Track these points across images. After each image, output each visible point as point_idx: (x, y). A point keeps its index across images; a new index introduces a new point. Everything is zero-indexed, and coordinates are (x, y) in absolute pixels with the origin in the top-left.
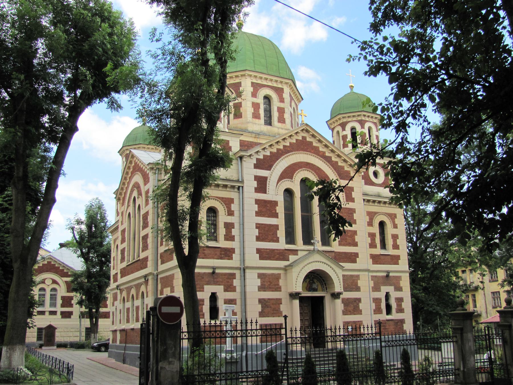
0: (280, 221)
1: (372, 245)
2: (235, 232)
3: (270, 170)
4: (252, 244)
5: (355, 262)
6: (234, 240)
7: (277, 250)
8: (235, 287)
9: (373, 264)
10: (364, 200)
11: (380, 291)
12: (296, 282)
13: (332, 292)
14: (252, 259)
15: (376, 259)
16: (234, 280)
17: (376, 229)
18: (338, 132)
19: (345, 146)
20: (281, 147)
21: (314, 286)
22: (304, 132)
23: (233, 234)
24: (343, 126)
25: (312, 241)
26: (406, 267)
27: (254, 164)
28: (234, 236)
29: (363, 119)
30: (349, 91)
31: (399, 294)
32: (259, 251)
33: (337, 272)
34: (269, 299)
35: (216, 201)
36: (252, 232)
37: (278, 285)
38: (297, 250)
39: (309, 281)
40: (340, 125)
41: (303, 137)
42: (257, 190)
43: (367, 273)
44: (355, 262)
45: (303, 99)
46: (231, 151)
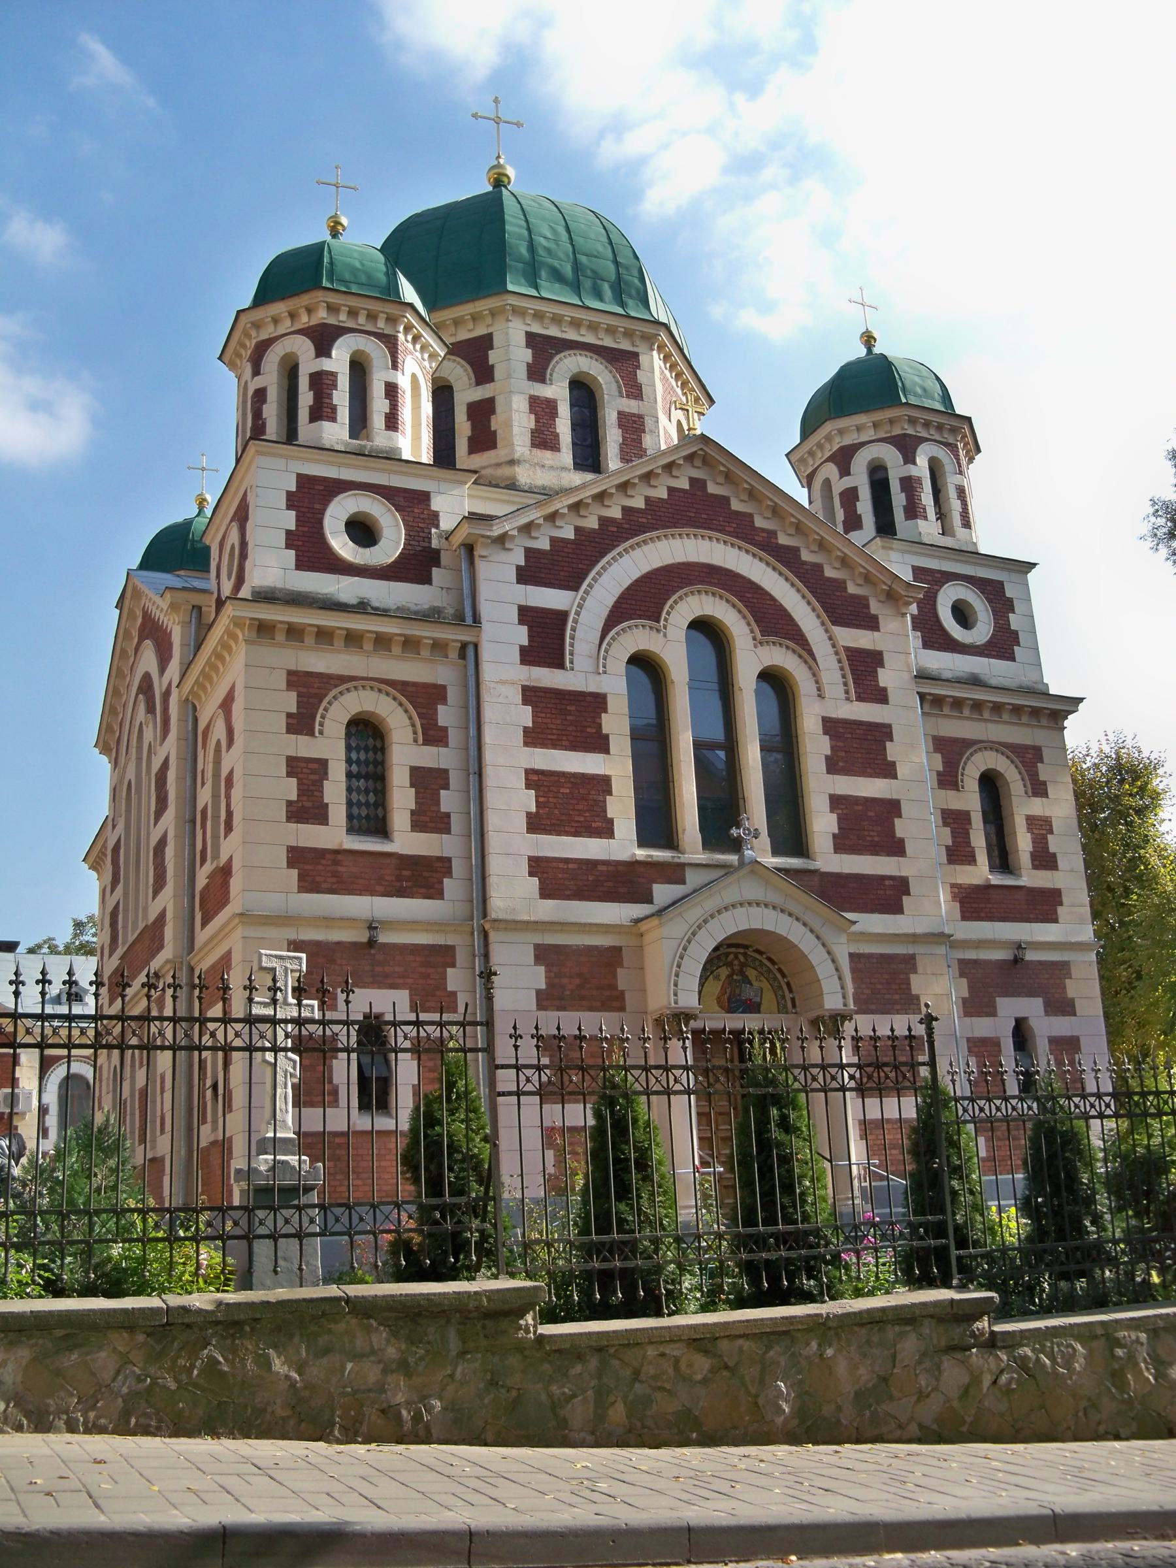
0: (617, 766)
1: (959, 853)
3: (576, 589)
4: (512, 841)
5: (898, 909)
6: (447, 830)
10: (922, 696)
11: (993, 1014)
12: (673, 972)
13: (813, 1014)
14: (513, 891)
15: (975, 903)
16: (450, 971)
17: (970, 799)
18: (827, 483)
19: (853, 522)
20: (616, 513)
21: (748, 993)
22: (698, 462)
23: (444, 809)
24: (843, 459)
25: (734, 832)
26: (1087, 933)
27: (519, 568)
28: (448, 815)
29: (911, 431)
30: (862, 352)
31: (1061, 1026)
32: (537, 866)
35: (383, 697)
36: (509, 802)
37: (614, 987)
38: (682, 866)
39: (729, 976)
40: (830, 459)
41: (692, 480)
42: (529, 656)
43: (942, 950)
45: (712, 401)
46: (437, 527)
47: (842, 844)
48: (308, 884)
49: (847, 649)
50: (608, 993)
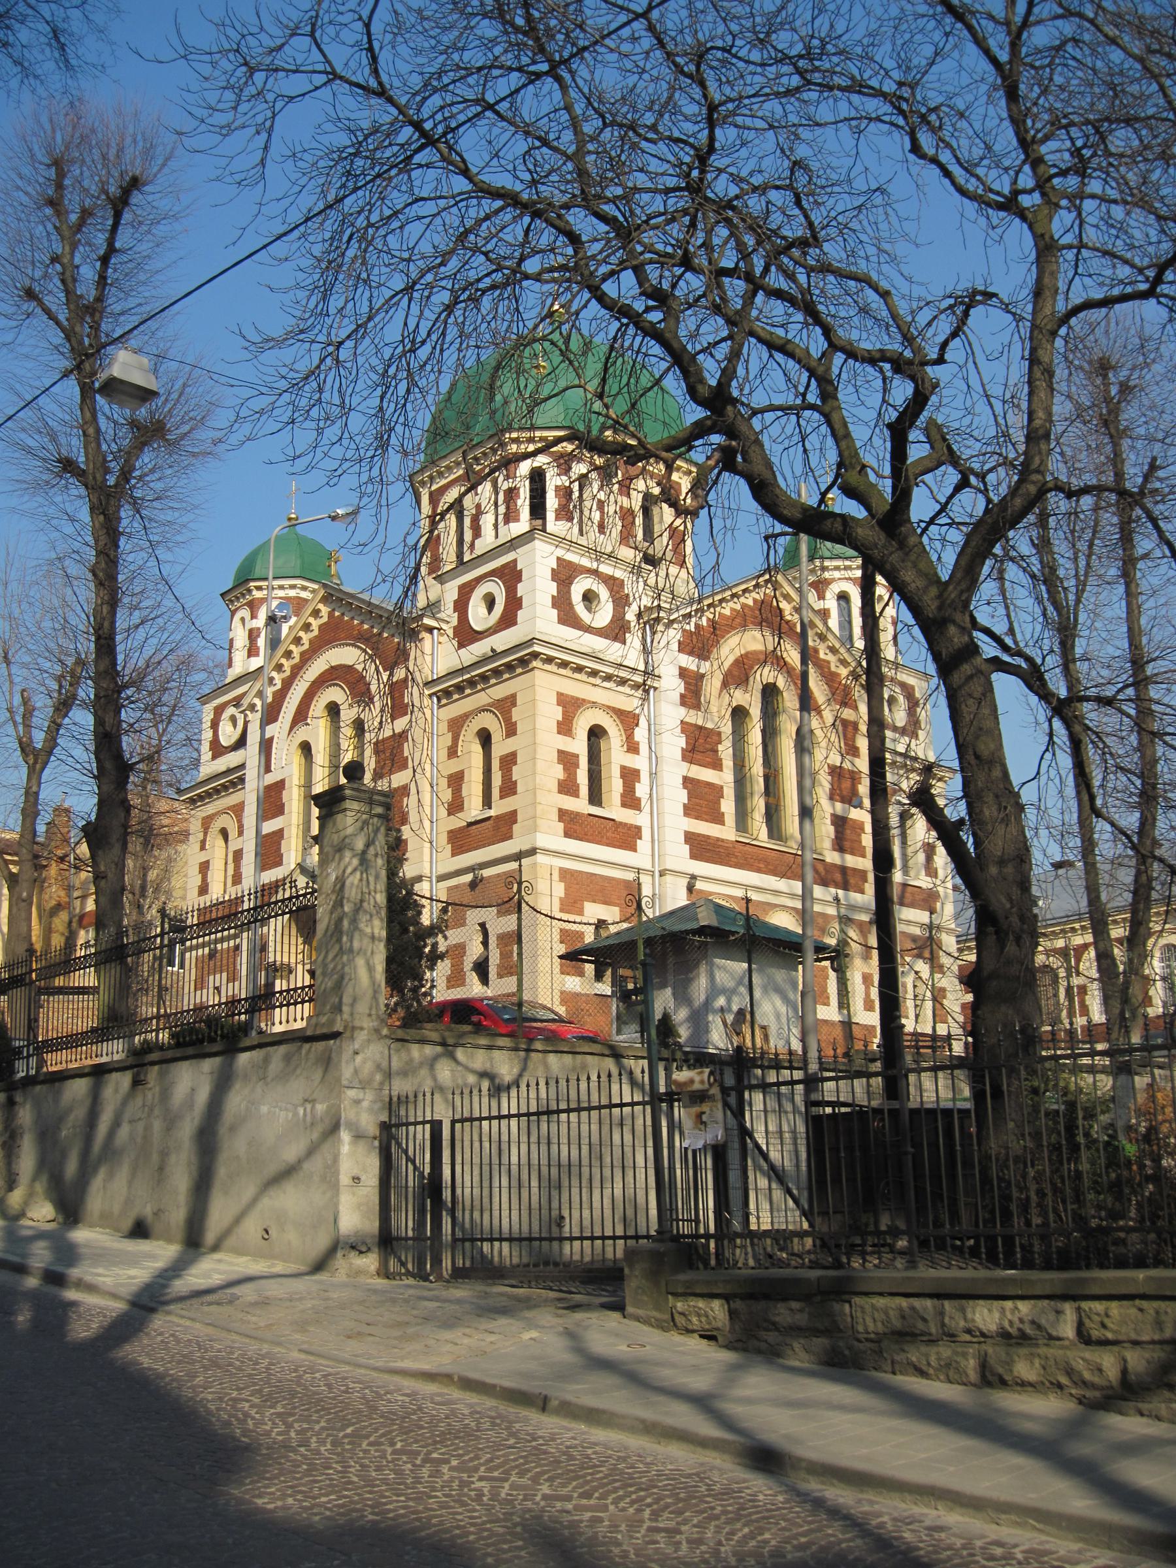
0: (725, 778)
2: (641, 790)
32: (690, 838)
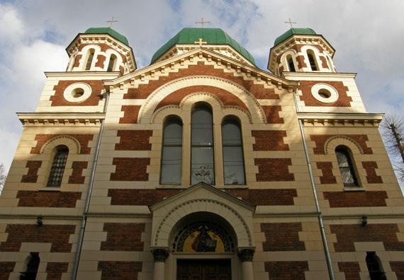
5: (291, 203)
7: (144, 190)
8: (71, 245)
9: (331, 206)
22: (201, 56)
28: (84, 177)
32: (112, 193)
33: (241, 215)
34: (118, 263)
37: (138, 240)
44: (291, 203)
47: (259, 178)
48: (22, 204)
49: (263, 106)
50: (135, 243)
